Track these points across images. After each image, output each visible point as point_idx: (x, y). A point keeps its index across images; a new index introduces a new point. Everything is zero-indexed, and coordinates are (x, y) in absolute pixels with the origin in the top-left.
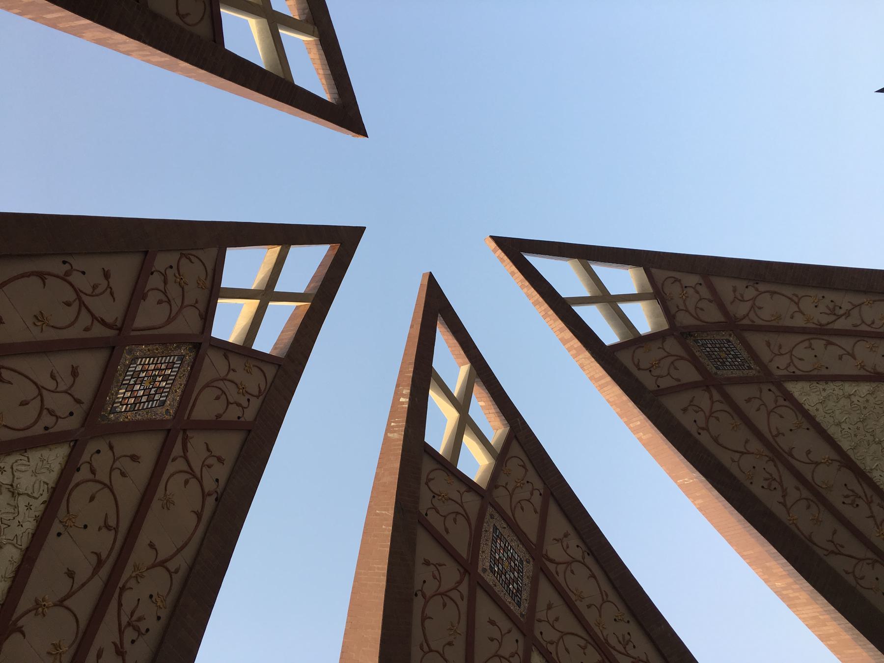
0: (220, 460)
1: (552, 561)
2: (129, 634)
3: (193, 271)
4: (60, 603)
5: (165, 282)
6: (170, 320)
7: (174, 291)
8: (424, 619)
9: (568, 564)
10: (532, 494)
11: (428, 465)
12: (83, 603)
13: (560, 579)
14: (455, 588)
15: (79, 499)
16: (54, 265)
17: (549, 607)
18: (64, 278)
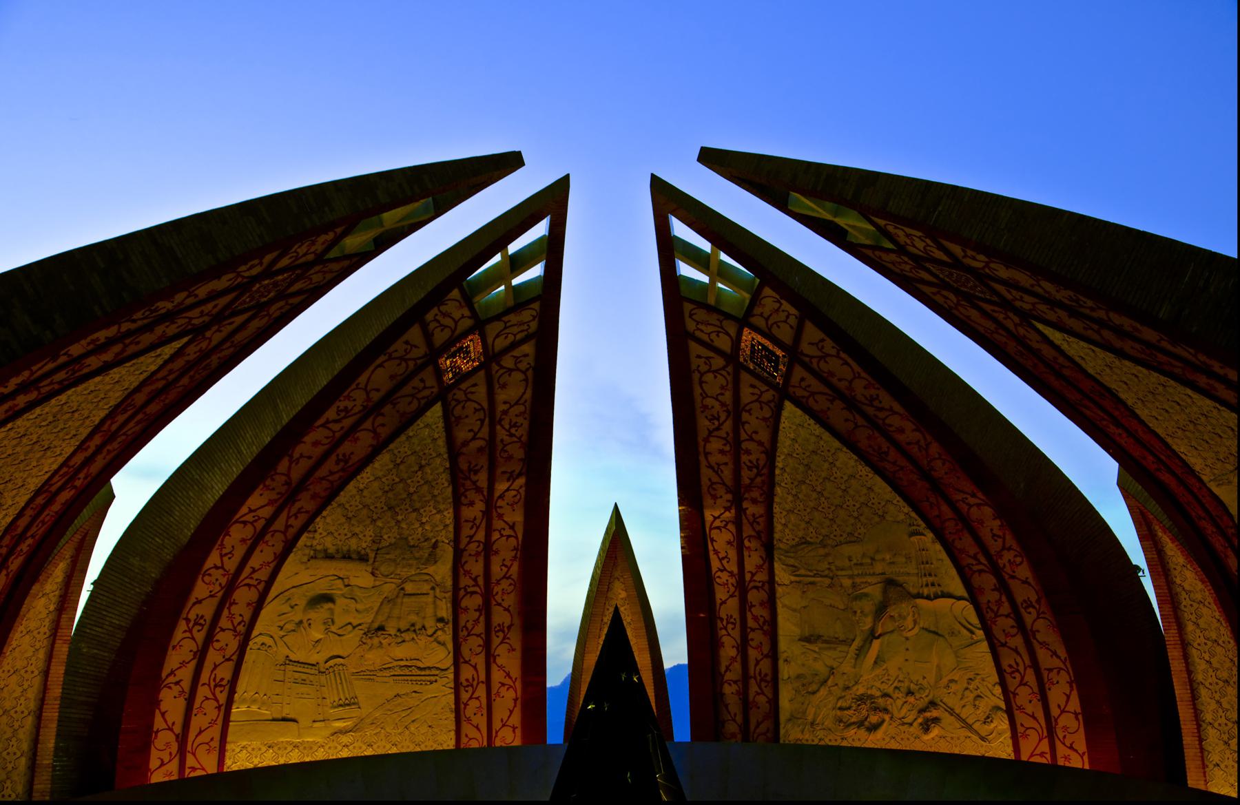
0: (526, 355)
1: (807, 356)
2: (513, 431)
3: (453, 306)
4: (474, 438)
5: (438, 321)
6: (453, 332)
7: (447, 322)
8: (701, 383)
9: (820, 358)
10: (788, 317)
11: (688, 307)
12: (485, 432)
13: (815, 365)
14: (724, 368)
15: (458, 411)
16: (382, 358)
17: (803, 379)
18: (390, 358)
